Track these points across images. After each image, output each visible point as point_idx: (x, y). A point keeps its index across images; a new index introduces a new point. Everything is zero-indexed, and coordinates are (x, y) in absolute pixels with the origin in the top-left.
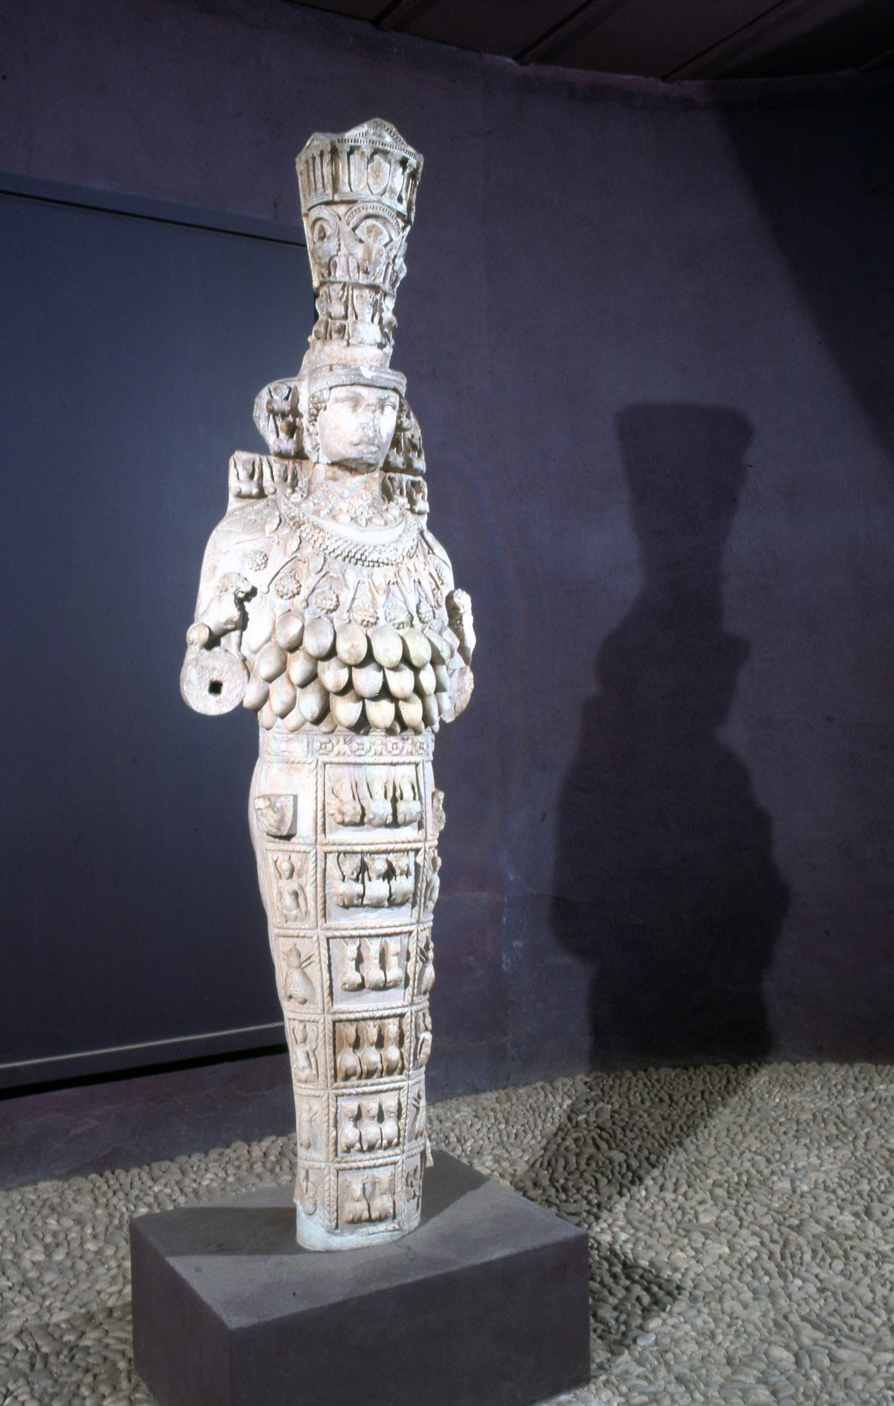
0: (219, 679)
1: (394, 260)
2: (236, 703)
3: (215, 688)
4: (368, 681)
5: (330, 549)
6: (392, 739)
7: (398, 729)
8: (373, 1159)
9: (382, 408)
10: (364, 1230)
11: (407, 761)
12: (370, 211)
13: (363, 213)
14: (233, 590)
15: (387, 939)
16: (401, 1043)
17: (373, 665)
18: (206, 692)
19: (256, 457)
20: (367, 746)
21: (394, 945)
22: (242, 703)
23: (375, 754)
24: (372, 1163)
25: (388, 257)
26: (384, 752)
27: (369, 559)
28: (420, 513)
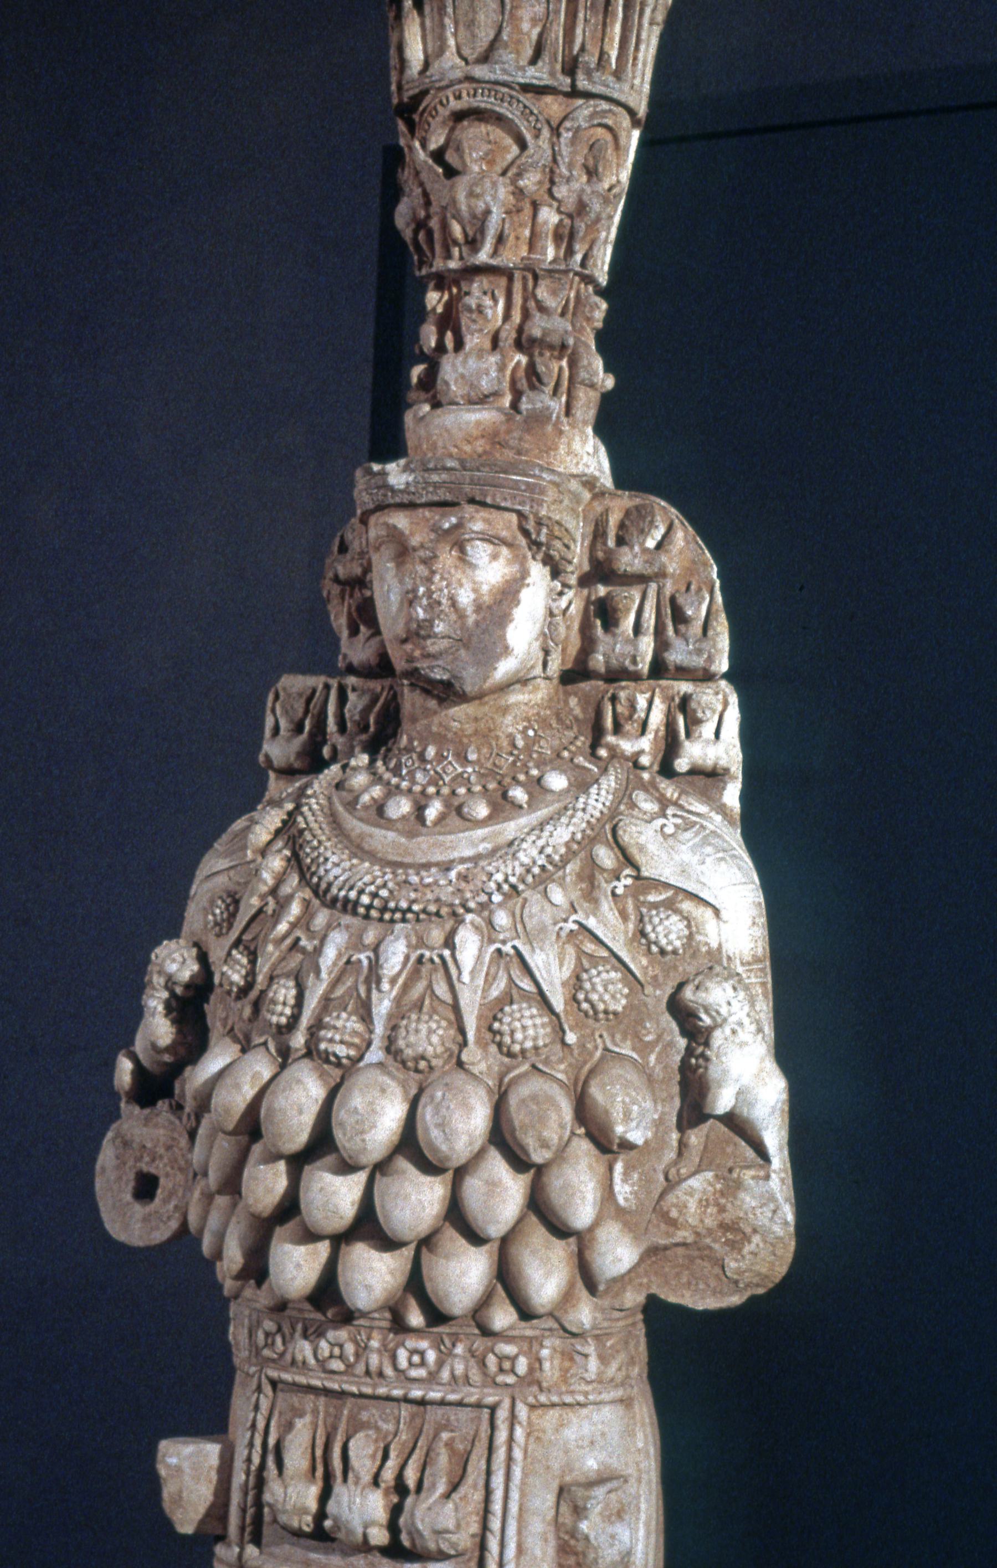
0: (153, 1170)
1: (550, 192)
2: (174, 1225)
3: (146, 1187)
4: (336, 1195)
5: (323, 886)
7: (416, 1318)
9: (461, 546)
11: (452, 1397)
12: (454, 105)
13: (444, 112)
14: (162, 981)
17: (330, 1159)
18: (128, 1197)
19: (317, 681)
20: (350, 1349)
22: (184, 1224)
23: (368, 1373)
25: (519, 193)
26: (389, 1371)
27: (392, 905)
28: (709, 777)
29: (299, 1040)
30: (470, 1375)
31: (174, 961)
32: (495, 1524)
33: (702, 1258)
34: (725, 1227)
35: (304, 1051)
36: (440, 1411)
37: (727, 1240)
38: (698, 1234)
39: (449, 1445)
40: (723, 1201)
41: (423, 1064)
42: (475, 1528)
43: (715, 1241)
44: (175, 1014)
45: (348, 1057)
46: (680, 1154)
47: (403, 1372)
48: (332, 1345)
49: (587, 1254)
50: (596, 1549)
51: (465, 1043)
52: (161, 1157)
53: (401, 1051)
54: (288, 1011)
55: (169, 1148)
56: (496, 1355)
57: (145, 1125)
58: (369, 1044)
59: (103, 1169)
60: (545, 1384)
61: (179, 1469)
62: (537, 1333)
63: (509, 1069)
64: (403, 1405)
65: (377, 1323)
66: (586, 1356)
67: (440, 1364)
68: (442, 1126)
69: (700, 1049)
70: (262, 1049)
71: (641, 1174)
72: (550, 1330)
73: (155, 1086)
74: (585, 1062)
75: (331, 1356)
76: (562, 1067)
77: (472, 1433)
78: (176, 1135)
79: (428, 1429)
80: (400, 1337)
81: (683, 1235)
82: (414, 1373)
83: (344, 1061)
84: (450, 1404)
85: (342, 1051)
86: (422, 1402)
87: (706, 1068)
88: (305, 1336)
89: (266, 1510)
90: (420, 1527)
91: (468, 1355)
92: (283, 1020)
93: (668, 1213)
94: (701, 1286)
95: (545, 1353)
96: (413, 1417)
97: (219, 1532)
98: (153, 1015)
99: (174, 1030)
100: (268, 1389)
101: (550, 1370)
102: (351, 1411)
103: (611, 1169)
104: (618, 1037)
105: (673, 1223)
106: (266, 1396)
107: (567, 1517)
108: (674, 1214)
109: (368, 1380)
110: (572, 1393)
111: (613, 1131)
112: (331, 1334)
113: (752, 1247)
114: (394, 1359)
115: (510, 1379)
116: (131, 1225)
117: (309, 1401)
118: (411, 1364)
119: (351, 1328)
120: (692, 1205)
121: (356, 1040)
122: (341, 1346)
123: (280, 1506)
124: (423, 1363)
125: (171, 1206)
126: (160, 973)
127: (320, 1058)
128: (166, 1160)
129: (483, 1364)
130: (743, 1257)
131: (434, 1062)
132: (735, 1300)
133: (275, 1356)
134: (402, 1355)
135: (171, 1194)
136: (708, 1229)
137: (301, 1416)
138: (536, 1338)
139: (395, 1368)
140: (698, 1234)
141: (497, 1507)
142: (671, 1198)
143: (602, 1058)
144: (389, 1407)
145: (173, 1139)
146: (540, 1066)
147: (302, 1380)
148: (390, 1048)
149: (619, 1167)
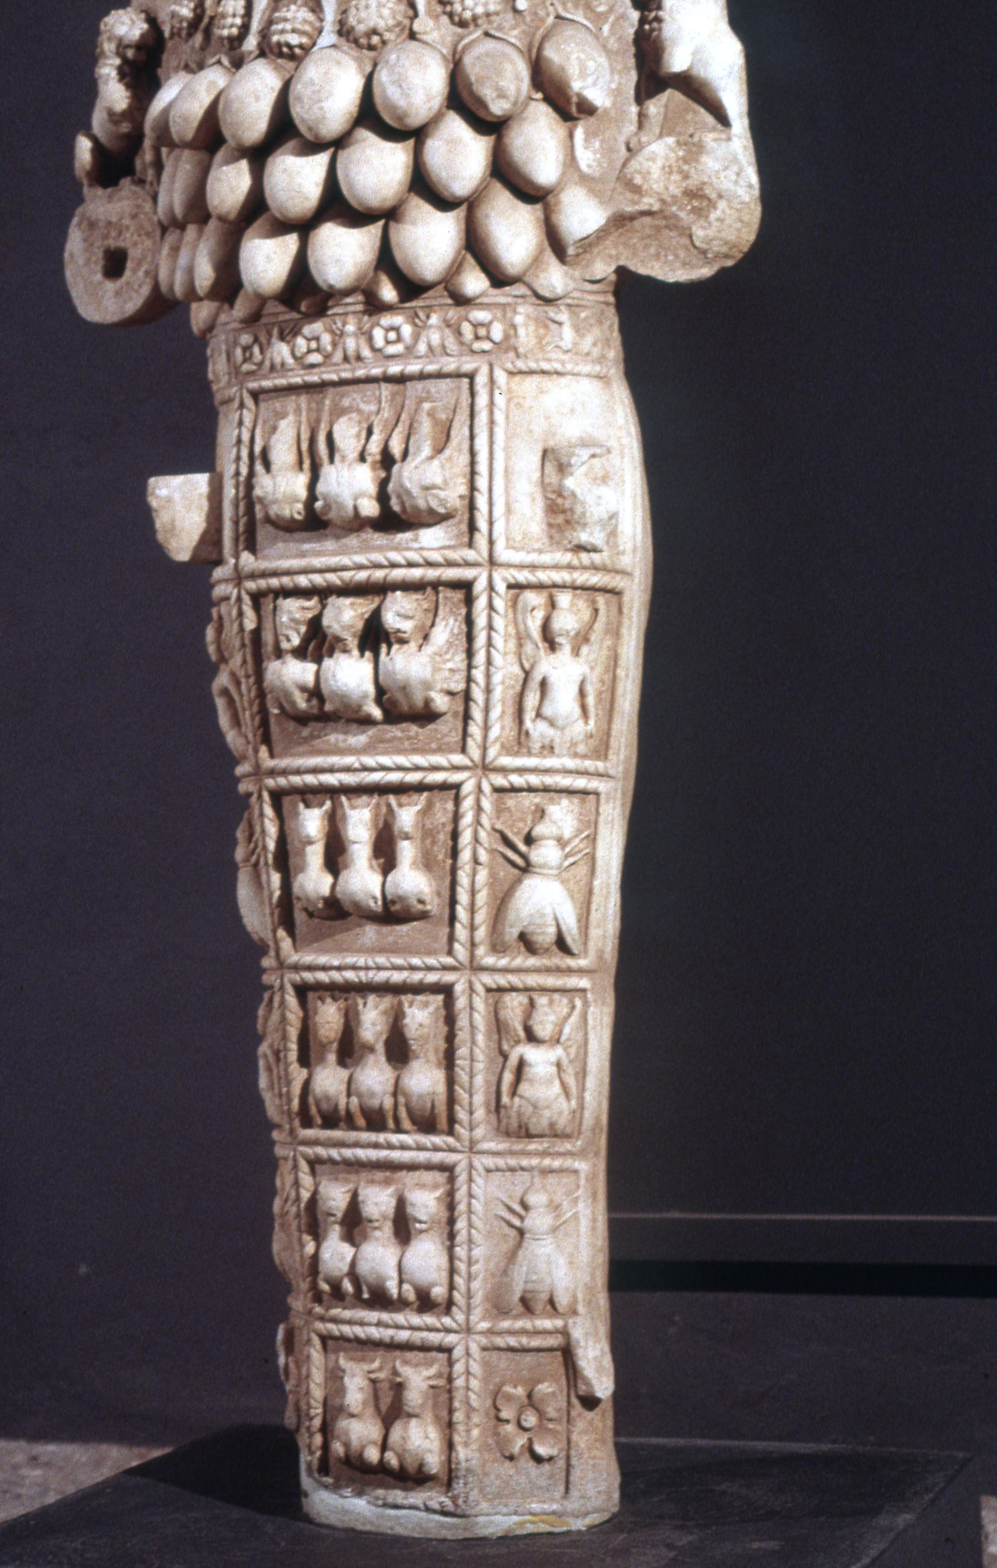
0: (121, 244)
2: (146, 291)
3: (115, 264)
6: (387, 320)
7: (388, 293)
8: (387, 1326)
10: (380, 1492)
11: (431, 368)
15: (392, 799)
16: (449, 1060)
17: (291, 144)
18: (99, 277)
21: (407, 816)
22: (156, 287)
23: (346, 359)
24: (386, 1334)
26: (366, 352)
29: (251, 43)
30: (447, 344)
31: (123, 24)
32: (482, 483)
33: (667, 227)
34: (691, 194)
35: (257, 52)
36: (420, 385)
37: (693, 208)
38: (663, 201)
39: (431, 414)
40: (686, 167)
41: (375, 40)
42: (463, 490)
43: (680, 209)
44: (127, 79)
45: (301, 46)
46: (641, 125)
47: (380, 350)
48: (309, 340)
49: (554, 218)
50: (583, 503)
51: (416, 15)
52: (128, 228)
53: (353, 28)
54: (238, 21)
55: (134, 216)
56: (470, 322)
57: (109, 202)
58: (320, 31)
59: (72, 255)
60: (521, 350)
61: (169, 500)
62: (510, 300)
63: (462, 38)
64: (384, 386)
65: (351, 308)
66: (560, 324)
67: (416, 337)
68: (398, 83)
69: (653, 14)
70: (217, 67)
71: (602, 142)
72: (523, 297)
73: (115, 166)
74: (538, 28)
75: (309, 351)
76: (515, 32)
77: (453, 402)
78: (140, 201)
79: (410, 404)
80: (375, 318)
81: (648, 202)
82: (391, 350)
83: (297, 51)
84: (430, 376)
85: (294, 40)
86: (401, 379)
87: (660, 30)
88: (282, 338)
89: (258, 508)
90: (408, 485)
91: (443, 326)
92: (235, 31)
93: (631, 180)
94: (671, 258)
95: (519, 319)
96: (394, 395)
97: (214, 557)
98: (106, 83)
99: (128, 94)
100: (249, 402)
101: (526, 337)
102: (333, 400)
103: (571, 136)
104: (570, 5)
105: (637, 190)
106: (249, 410)
107: (552, 476)
108: (638, 180)
109: (347, 366)
110: (549, 360)
111: (570, 87)
112: (307, 330)
113: (718, 213)
114: (370, 339)
115: (487, 346)
116: (102, 302)
117: (291, 402)
118: (388, 342)
119: (325, 319)
120: (655, 170)
121: (307, 28)
122: (317, 339)
123: (270, 497)
124: (399, 339)
125: (141, 274)
126: (110, 39)
127: (272, 52)
128: (132, 229)
129: (459, 333)
130: (710, 223)
131: (387, 36)
132: (706, 272)
133: (254, 367)
134: (378, 334)
135: (139, 264)
136: (673, 196)
137: (283, 416)
138: (509, 304)
139: (374, 349)
140: (663, 201)
141: (482, 467)
142: (634, 165)
143: (554, 25)
144: (370, 389)
145: (138, 206)
146: (493, 32)
147: (282, 382)
148: (344, 31)
149: (579, 133)
